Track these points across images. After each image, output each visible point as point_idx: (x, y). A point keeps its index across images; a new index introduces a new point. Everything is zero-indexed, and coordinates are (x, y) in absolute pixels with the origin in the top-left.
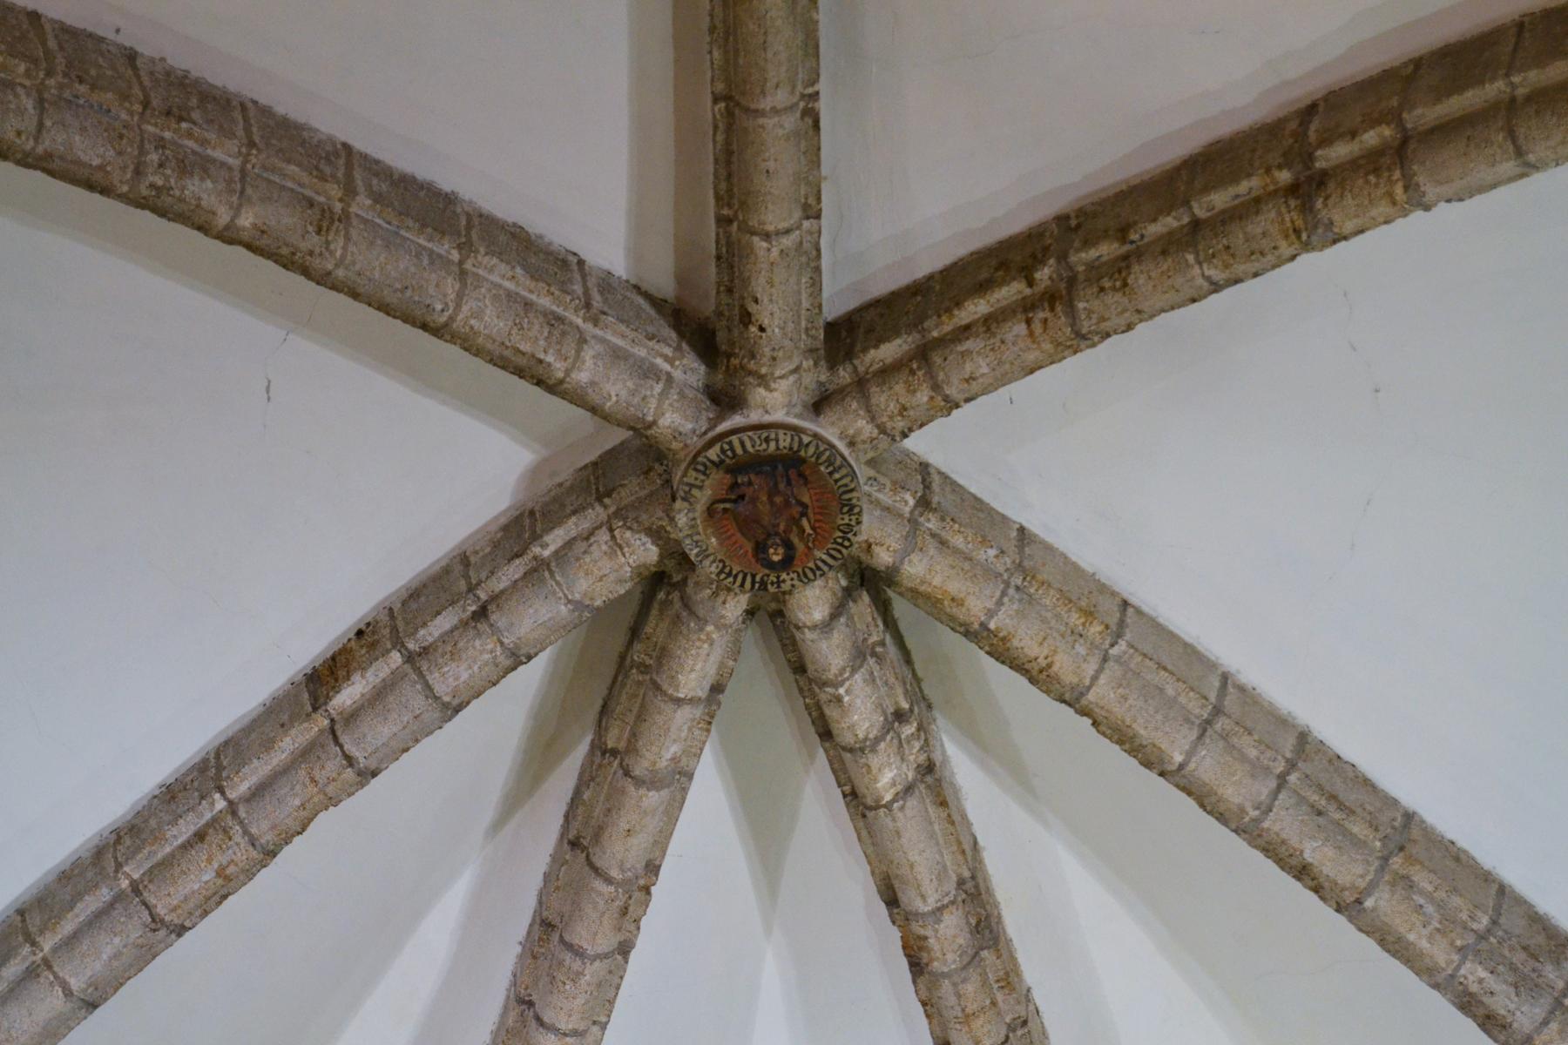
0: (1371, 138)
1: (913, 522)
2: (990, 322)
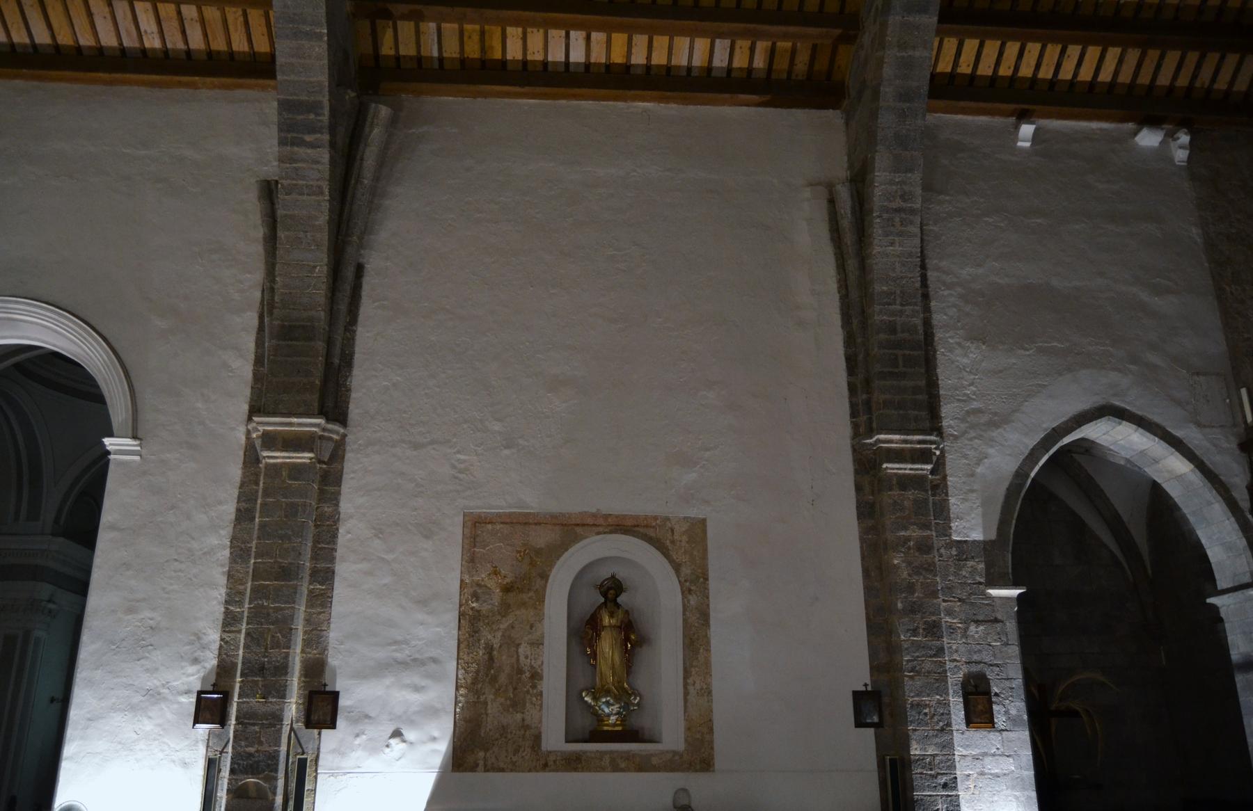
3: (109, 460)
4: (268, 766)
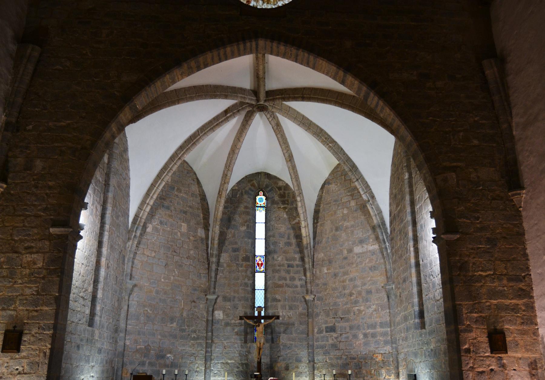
0: (308, 96)
1: (273, 106)
2: (279, 98)
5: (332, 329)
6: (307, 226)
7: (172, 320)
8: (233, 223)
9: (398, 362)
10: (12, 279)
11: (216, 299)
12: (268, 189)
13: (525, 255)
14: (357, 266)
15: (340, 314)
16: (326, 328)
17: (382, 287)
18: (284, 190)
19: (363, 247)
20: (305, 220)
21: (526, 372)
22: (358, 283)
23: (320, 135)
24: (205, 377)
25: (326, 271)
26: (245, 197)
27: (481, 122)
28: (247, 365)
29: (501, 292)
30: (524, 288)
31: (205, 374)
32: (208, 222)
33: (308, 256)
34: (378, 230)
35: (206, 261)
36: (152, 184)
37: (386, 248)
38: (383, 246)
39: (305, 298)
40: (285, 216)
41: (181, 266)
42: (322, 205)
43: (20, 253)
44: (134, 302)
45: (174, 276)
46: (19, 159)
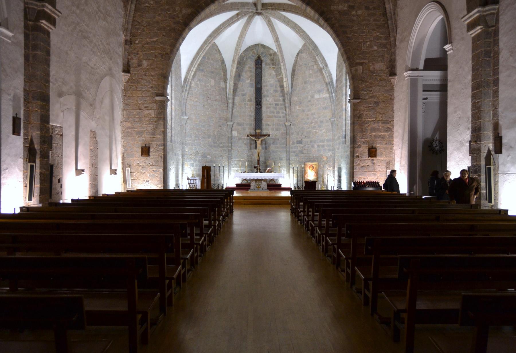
2: (270, 9)
3: (447, 54)
4: (479, 170)
5: (300, 142)
6: (287, 81)
7: (209, 137)
8: (242, 77)
9: (334, 161)
10: (141, 122)
11: (233, 125)
12: (263, 55)
13: (393, 110)
14: (316, 106)
15: (305, 134)
16: (297, 141)
17: (329, 119)
18: (274, 55)
19: (320, 95)
20: (286, 77)
21: (384, 166)
22: (316, 116)
23: (295, 28)
24: (228, 168)
25: (298, 108)
26: (249, 60)
27: (380, 36)
28: (251, 161)
29: (378, 129)
30: (390, 127)
31: (228, 166)
32: (226, 78)
33: (288, 99)
34: (329, 86)
35: (226, 102)
36: (194, 58)
37: (333, 97)
38: (331, 96)
39: (285, 124)
40: (274, 73)
41: (212, 106)
42: (297, 67)
43: (143, 110)
44: (188, 128)
45: (208, 112)
46: (134, 60)
